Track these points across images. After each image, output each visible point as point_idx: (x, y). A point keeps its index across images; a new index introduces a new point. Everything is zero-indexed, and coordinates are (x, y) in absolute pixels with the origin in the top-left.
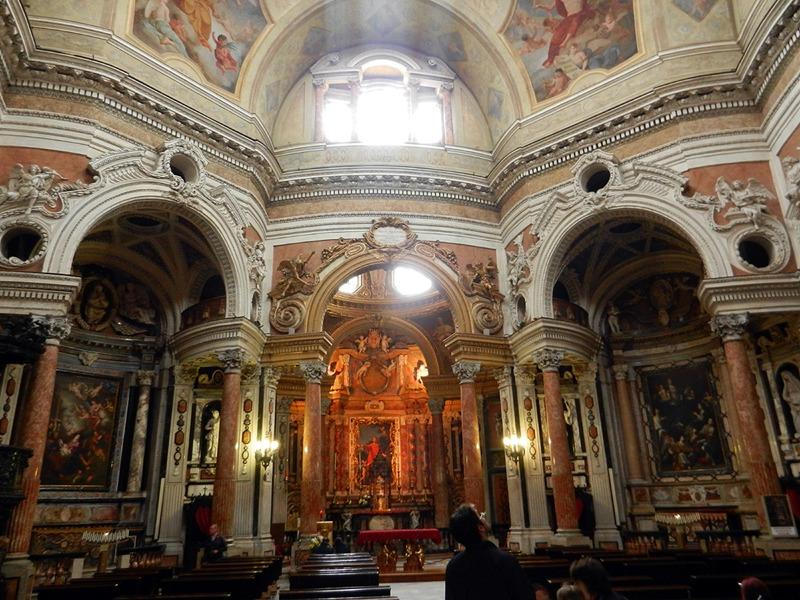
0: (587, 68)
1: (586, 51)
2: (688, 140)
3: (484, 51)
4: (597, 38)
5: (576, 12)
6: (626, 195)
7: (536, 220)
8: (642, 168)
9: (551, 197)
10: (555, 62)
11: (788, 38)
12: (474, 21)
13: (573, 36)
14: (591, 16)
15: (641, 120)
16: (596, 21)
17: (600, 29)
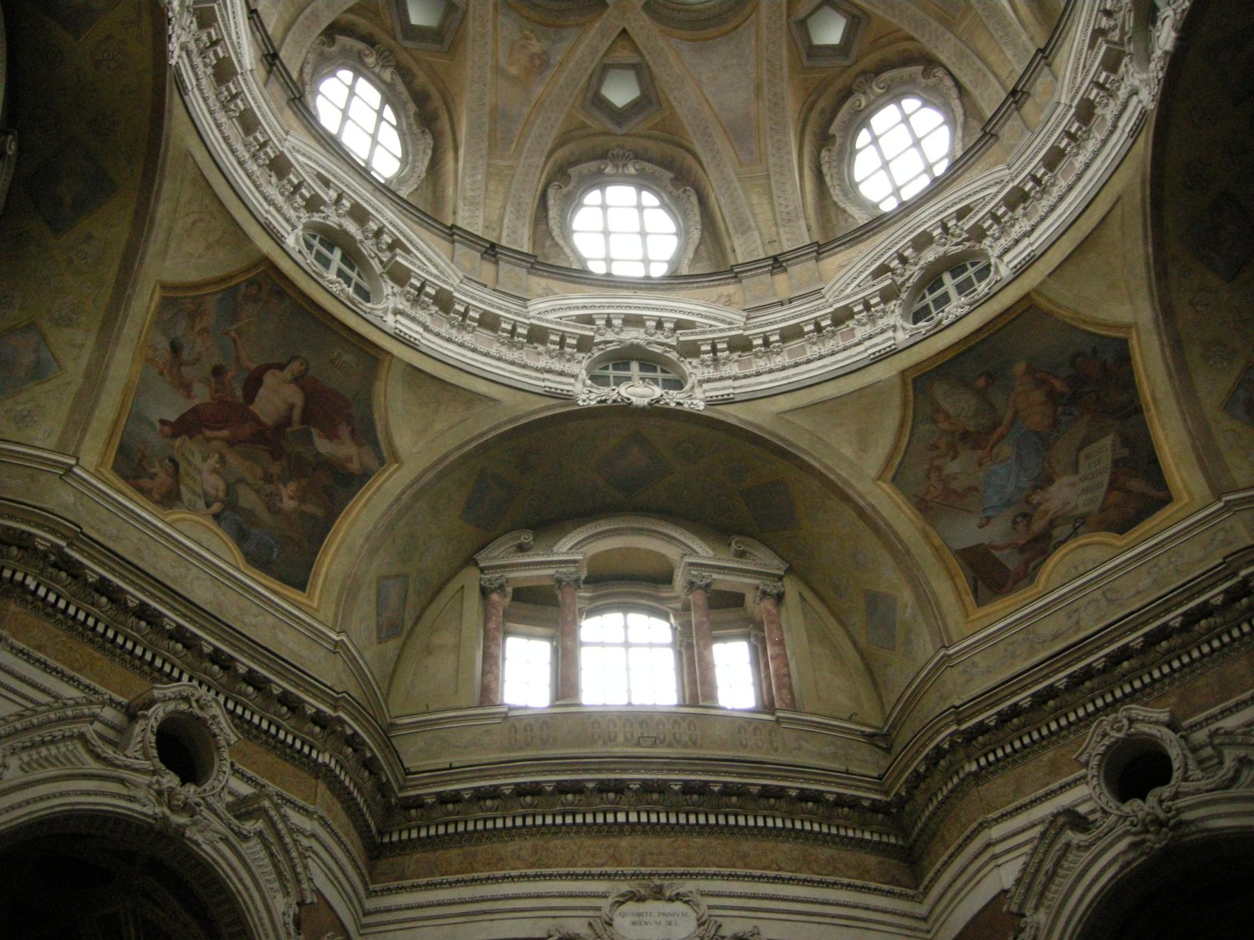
0: (216, 517)
1: (229, 490)
2: (325, 825)
3: (111, 272)
4: (257, 492)
5: (263, 418)
6: (225, 840)
7: (21, 716)
8: (273, 813)
9: (91, 703)
10: (178, 442)
11: (530, 810)
12: (158, 216)
13: (231, 443)
14: (277, 454)
15: (280, 716)
16: (275, 469)
17: (269, 488)
